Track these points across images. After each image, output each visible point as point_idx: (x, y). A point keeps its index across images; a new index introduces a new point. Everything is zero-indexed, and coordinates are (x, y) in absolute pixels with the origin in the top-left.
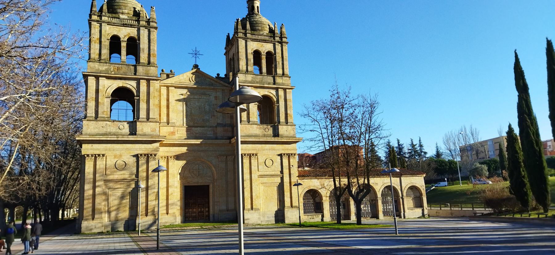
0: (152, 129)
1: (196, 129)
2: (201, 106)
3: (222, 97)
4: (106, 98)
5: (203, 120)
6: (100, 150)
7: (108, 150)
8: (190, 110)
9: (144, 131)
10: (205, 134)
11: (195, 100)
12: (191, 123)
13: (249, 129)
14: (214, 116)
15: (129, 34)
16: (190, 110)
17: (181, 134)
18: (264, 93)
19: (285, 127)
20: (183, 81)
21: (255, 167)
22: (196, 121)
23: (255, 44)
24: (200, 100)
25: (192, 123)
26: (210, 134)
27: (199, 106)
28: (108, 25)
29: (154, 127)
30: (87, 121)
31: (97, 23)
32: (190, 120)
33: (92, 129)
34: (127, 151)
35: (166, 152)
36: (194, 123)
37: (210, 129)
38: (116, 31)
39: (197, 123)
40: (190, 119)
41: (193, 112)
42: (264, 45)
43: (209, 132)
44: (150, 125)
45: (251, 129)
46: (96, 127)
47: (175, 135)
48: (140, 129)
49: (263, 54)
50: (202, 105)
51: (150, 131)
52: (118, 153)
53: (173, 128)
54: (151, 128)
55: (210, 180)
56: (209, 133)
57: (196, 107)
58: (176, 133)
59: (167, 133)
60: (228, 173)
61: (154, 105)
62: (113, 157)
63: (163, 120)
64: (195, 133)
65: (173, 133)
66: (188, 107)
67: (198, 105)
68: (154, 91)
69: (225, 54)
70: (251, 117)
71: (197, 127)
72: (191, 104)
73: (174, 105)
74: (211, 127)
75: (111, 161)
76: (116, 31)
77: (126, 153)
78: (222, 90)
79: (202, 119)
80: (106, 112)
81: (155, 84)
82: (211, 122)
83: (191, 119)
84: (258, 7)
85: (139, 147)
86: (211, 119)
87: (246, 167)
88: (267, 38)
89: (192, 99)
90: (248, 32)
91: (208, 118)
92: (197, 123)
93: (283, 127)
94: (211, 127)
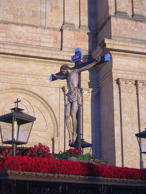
1: (19, 28)
10: (36, 41)
12: (8, 16)
14: (57, 7)
26: (46, 42)
32: (7, 10)
37: (47, 32)
43: (46, 38)
45: (136, 29)
55: (43, 137)
56: (44, 40)
64: (16, 36)
70: (136, 8)
71: (22, 25)
74: (49, 28)
79: (33, 11)
82: (50, 18)
83: (10, 8)
86: (50, 14)
87: (126, 109)
91: (43, 10)
94: (49, 28)
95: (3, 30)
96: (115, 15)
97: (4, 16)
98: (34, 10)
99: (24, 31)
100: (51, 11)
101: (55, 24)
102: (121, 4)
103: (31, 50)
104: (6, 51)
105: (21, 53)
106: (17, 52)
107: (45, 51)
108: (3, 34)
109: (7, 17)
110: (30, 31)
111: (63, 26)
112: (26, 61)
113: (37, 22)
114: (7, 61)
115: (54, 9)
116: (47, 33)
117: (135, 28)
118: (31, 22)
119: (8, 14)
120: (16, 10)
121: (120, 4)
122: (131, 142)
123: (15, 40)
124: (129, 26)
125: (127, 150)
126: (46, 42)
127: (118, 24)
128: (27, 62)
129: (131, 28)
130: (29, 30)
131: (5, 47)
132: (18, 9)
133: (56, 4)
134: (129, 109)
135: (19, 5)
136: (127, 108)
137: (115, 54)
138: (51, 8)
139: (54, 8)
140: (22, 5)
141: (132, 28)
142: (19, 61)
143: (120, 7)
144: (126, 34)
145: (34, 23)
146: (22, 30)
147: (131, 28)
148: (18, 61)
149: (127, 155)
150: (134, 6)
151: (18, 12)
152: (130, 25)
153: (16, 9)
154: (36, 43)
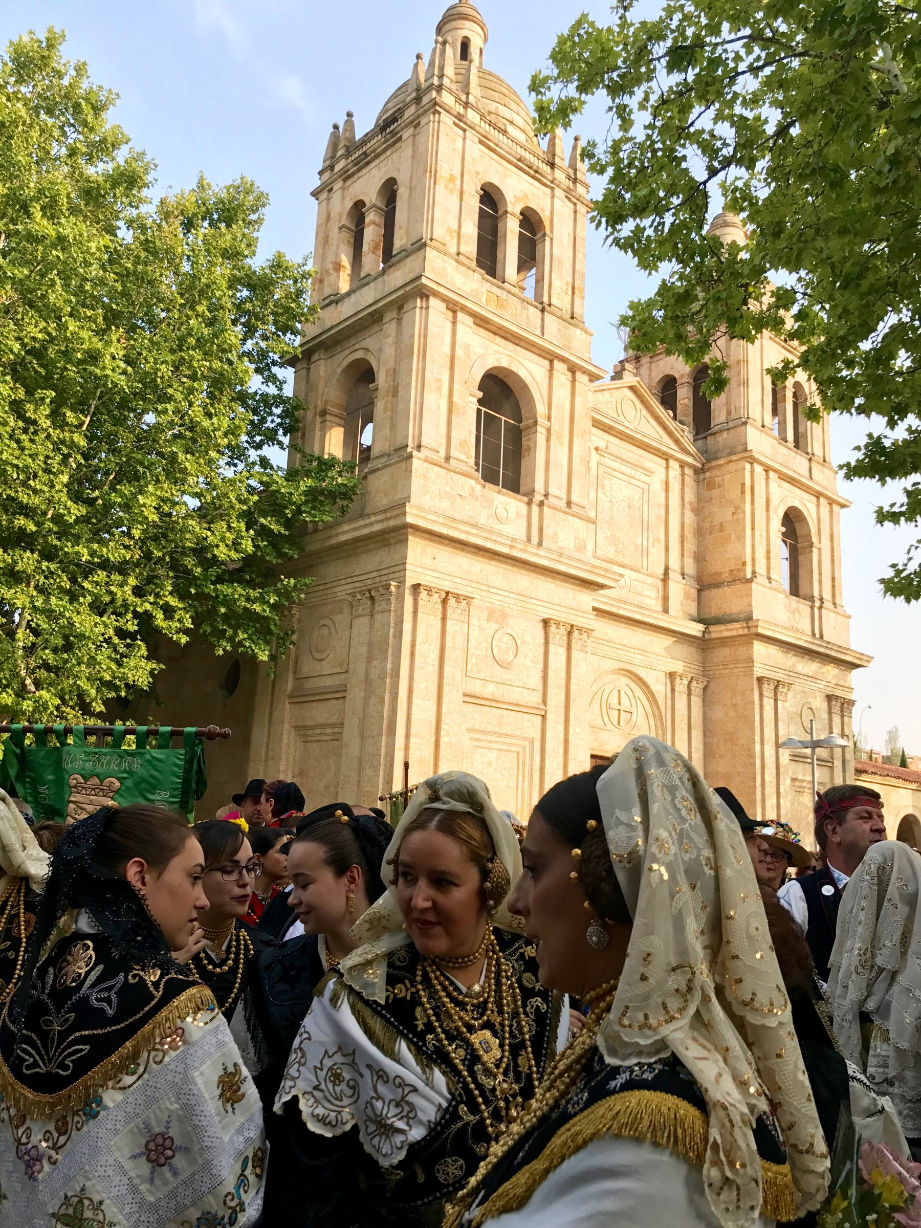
7: (475, 585)
9: (560, 544)
14: (658, 539)
24: (633, 481)
28: (481, 142)
31: (455, 124)
34: (519, 603)
41: (616, 514)
51: (572, 547)
56: (646, 593)
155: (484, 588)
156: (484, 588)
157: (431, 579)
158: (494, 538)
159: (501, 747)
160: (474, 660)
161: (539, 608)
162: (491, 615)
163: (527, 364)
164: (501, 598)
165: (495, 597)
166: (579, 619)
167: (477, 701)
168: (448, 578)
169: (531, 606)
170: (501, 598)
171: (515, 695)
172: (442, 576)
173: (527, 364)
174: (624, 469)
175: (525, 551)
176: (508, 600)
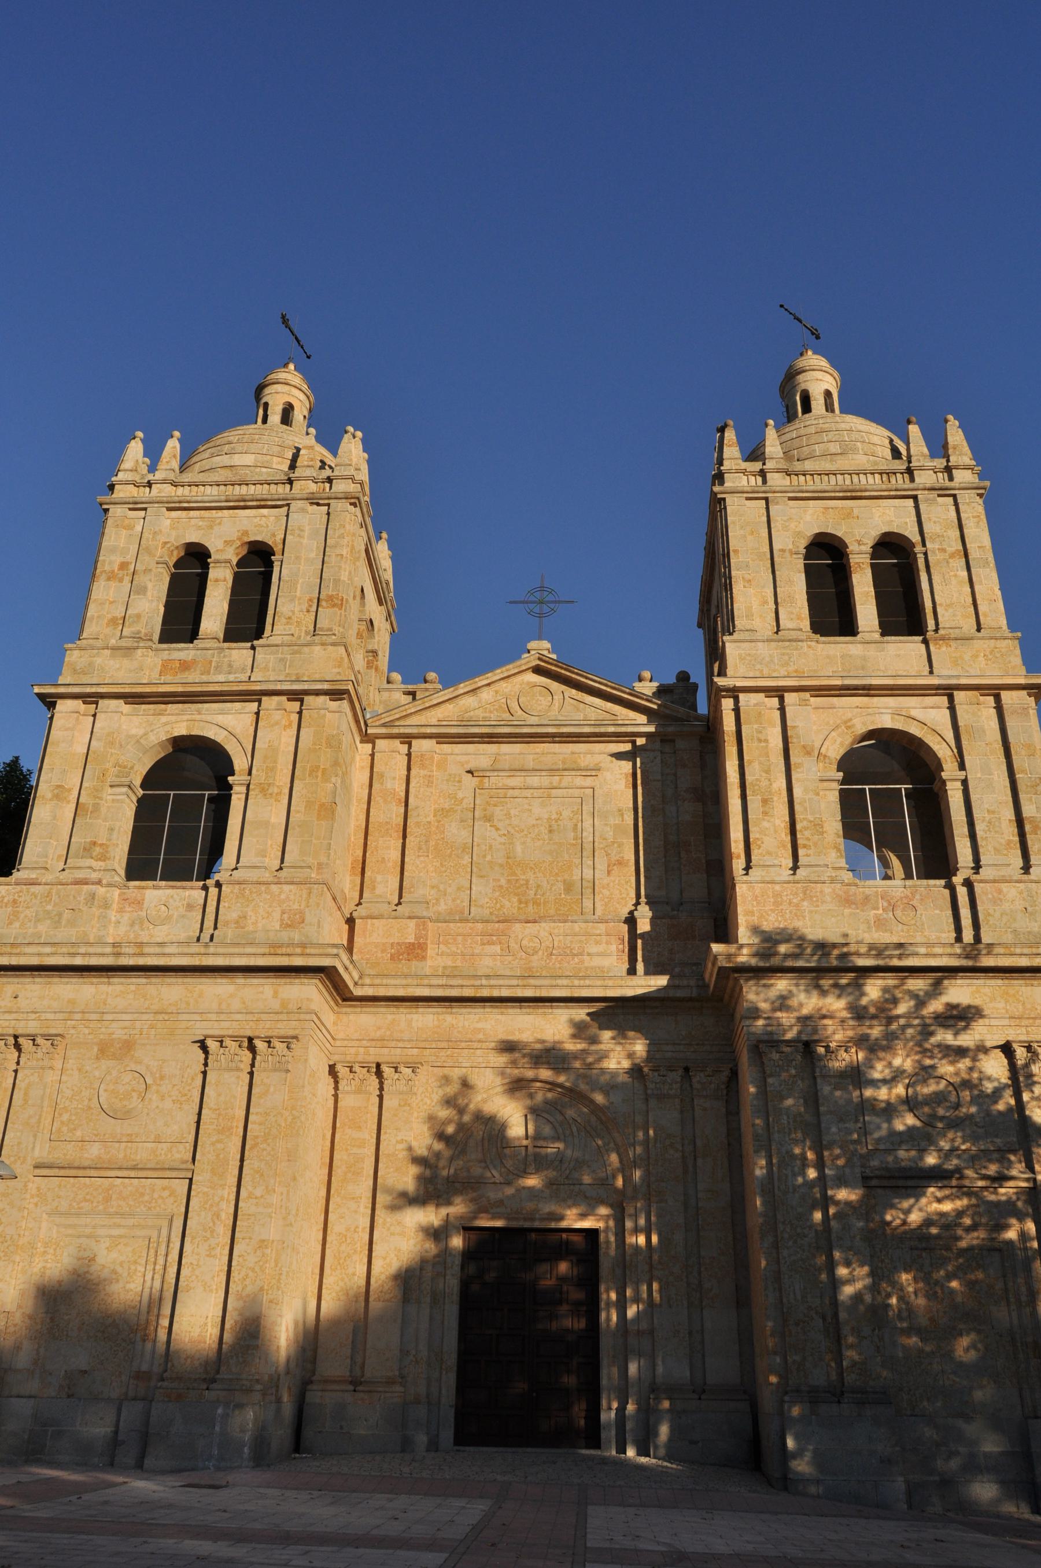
0: (286, 916)
2: (557, 820)
3: (662, 775)
4: (111, 786)
5: (568, 887)
6: (43, 1016)
8: (503, 840)
11: (528, 793)
13: (797, 905)
15: (246, 533)
16: (503, 840)
17: (454, 954)
18: (873, 722)
19: (1011, 891)
20: (480, 714)
21: (841, 1120)
22: (532, 893)
23: (810, 511)
25: (515, 900)
26: (599, 954)
27: (549, 819)
29: (296, 906)
30: (17, 884)
32: (501, 887)
33: (30, 921)
34: (159, 1025)
35: (374, 1043)
36: (520, 902)
38: (199, 528)
39: (536, 903)
40: (503, 882)
41: (519, 849)
42: (856, 511)
43: (597, 943)
44: (283, 896)
46: (48, 912)
47: (424, 958)
48: (234, 915)
49: (852, 547)
50: (566, 814)
51: (277, 926)
52: (118, 1032)
53: (417, 925)
54: (283, 913)
56: (594, 949)
57: (534, 826)
58: (430, 952)
59: (383, 951)
60: (700, 1161)
61: (309, 804)
62: (96, 1049)
63: (374, 888)
65: (415, 950)
66: (497, 829)
67: (546, 816)
68: (314, 744)
69: (699, 627)
70: (805, 846)
72: (512, 812)
73: (431, 818)
75: (80, 1070)
76: (199, 528)
77: (153, 1032)
78: (662, 741)
80: (101, 845)
81: (324, 716)
82: (606, 892)
83: (509, 881)
84: (828, 394)
85: (220, 1004)
88: (874, 481)
89: (516, 793)
90: (770, 465)
92: (536, 903)
93: (1000, 891)
95: (494, 938)
96: (747, 874)
97: (496, 903)
98: (566, 877)
99: (543, 934)
100: (609, 872)
101: (617, 906)
102: (763, 843)
103: (554, 983)
104: (496, 993)
105: (529, 993)
106: (520, 993)
107: (587, 982)
108: (493, 947)
109: (501, 906)
110: (556, 931)
111: (636, 910)
112: (546, 1010)
113: (575, 907)
114: (502, 1014)
115: (615, 867)
116: (598, 932)
117: (803, 900)
118: (560, 910)
119: (503, 897)
120: (522, 885)
121: (759, 843)
122: (800, 1210)
123: (521, 959)
124: (785, 898)
125: (788, 1230)
126: (599, 954)
127: (757, 896)
128: (550, 1011)
129: (790, 903)
130: (554, 928)
131: (493, 982)
132: (527, 881)
133: (620, 853)
134: (791, 1121)
135: (528, 870)
136: (785, 1117)
137: (748, 980)
138: (609, 866)
139: (615, 865)
140: (537, 870)
141: (795, 901)
142: (531, 1010)
143: (760, 851)
144: (777, 920)
145: (566, 909)
146: (539, 932)
147: (790, 903)
148: (528, 1010)
149: (791, 1243)
150: (800, 842)
151: (527, 888)
152: (787, 895)
153: (522, 882)
154: (573, 959)
155: (94, 1017)
156: (94, 1017)
157: (7, 1024)
158: (82, 950)
159: (116, 1232)
160: (65, 1117)
161: (198, 1025)
162: (104, 1050)
163: (220, 719)
164: (127, 1024)
165: (114, 1025)
166: (280, 1025)
167: (62, 1172)
168: (33, 1016)
169: (184, 1025)
170: (127, 1024)
171: (142, 1153)
172: (21, 1016)
173: (220, 719)
174: (534, 780)
175: (142, 954)
176: (138, 1024)
